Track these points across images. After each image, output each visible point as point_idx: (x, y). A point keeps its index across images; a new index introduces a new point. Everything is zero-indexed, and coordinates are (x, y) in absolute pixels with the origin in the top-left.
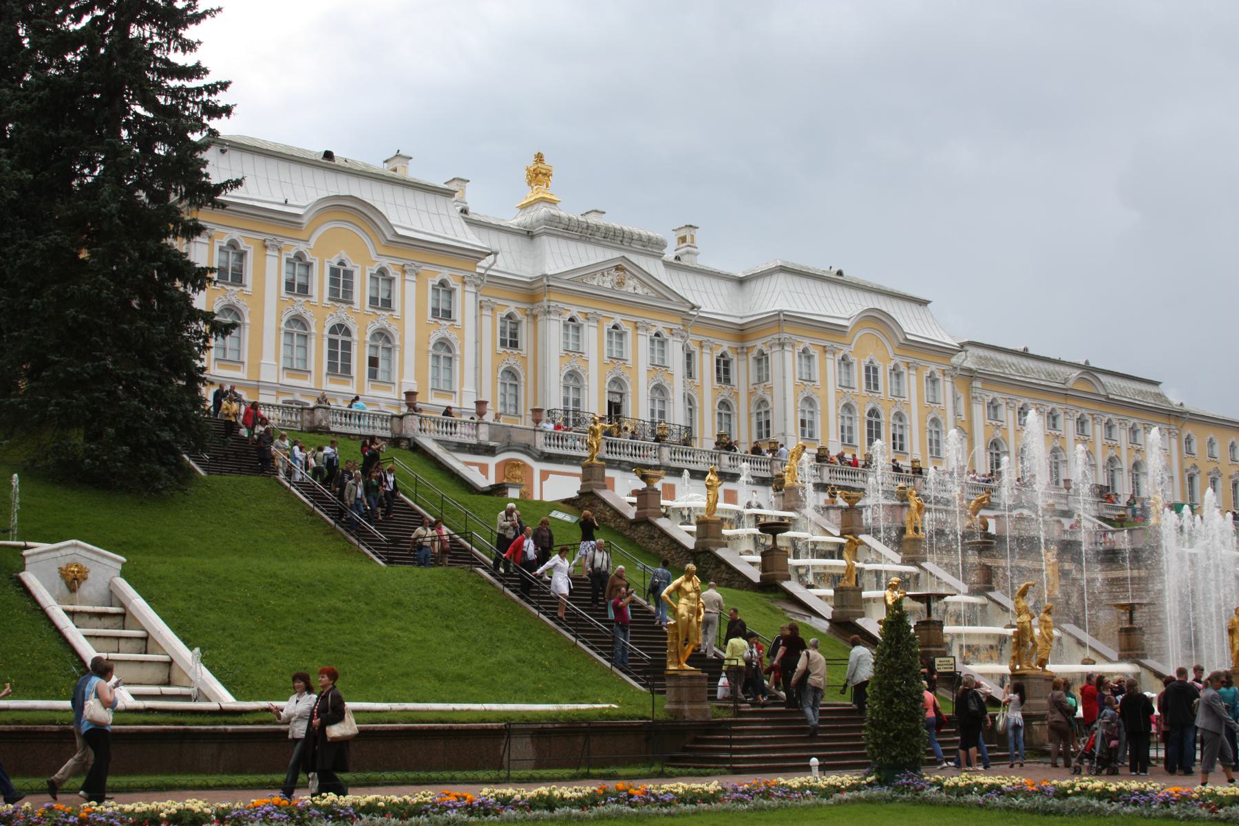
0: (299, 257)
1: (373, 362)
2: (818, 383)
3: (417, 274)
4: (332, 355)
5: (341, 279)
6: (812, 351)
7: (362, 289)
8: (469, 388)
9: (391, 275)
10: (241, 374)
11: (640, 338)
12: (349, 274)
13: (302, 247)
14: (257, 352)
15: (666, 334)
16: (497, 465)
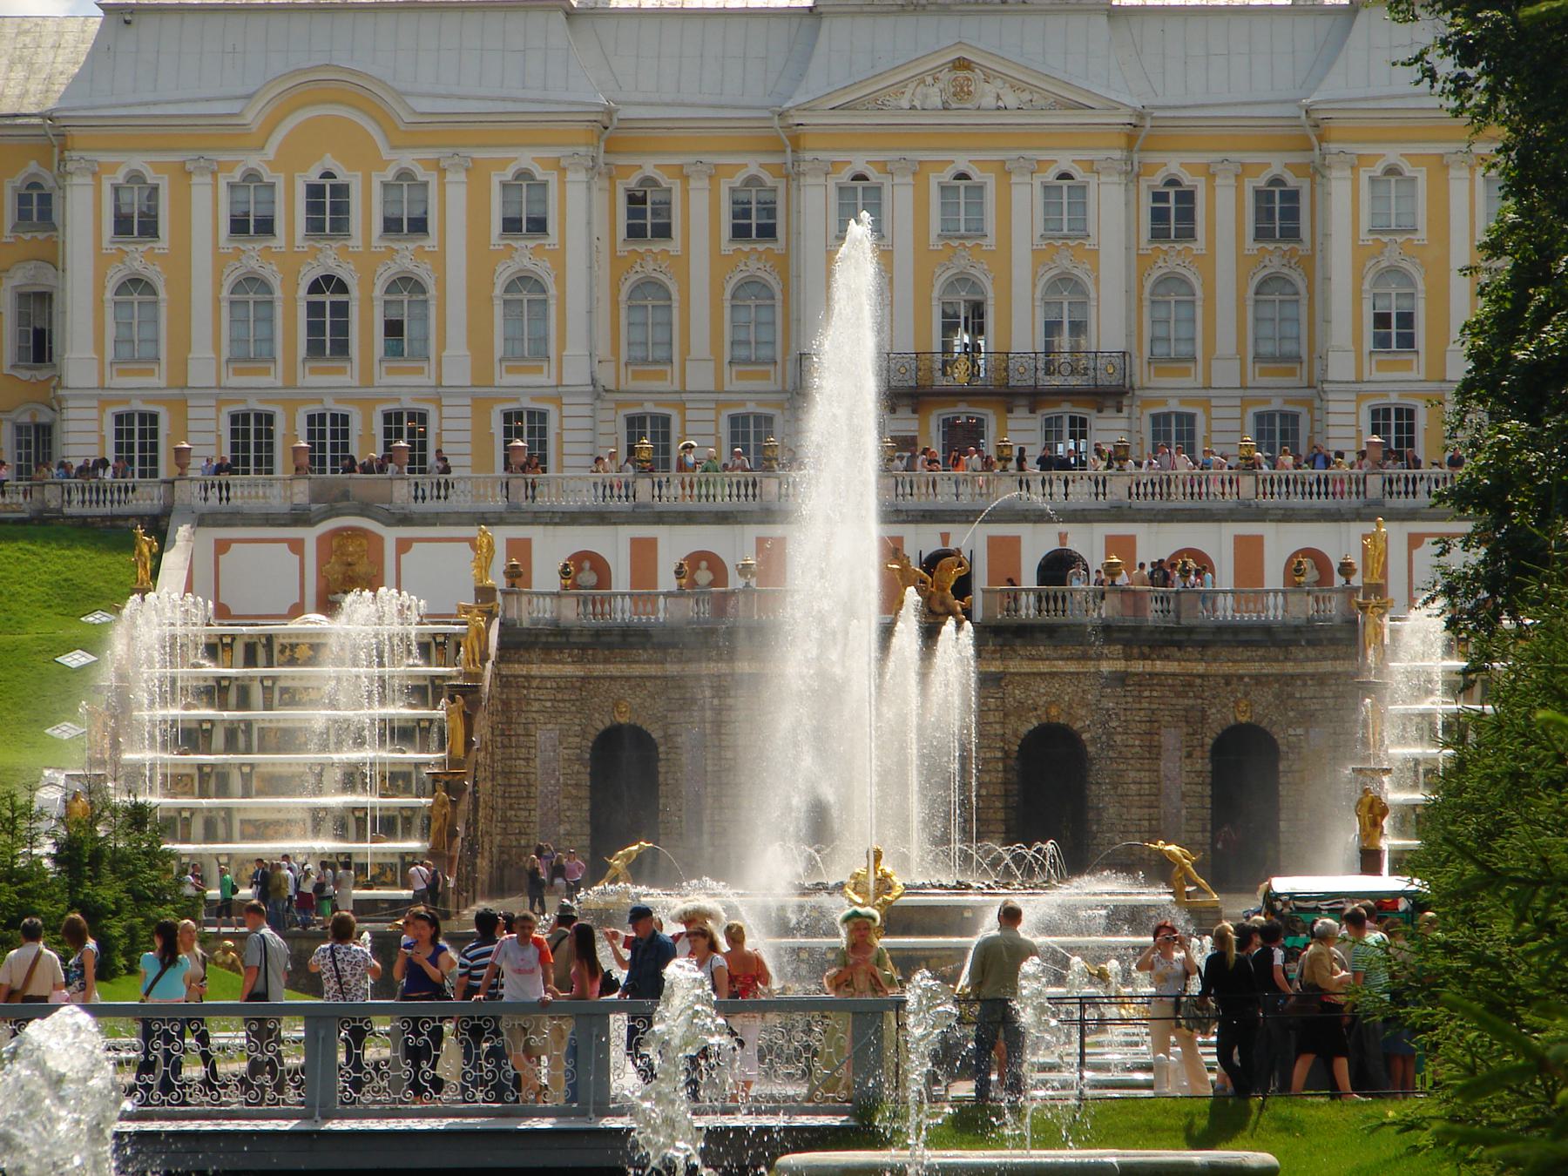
0: (252, 176)
1: (394, 329)
2: (1422, 235)
3: (467, 170)
4: (315, 328)
5: (328, 200)
6: (1408, 170)
7: (366, 212)
8: (576, 348)
9: (420, 178)
10: (158, 380)
11: (1016, 191)
12: (341, 191)
13: (254, 161)
14: (182, 342)
15: (1079, 175)
16: (321, 540)
